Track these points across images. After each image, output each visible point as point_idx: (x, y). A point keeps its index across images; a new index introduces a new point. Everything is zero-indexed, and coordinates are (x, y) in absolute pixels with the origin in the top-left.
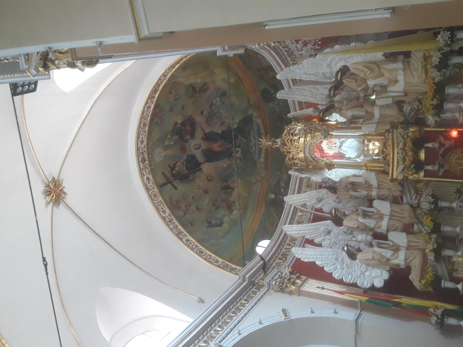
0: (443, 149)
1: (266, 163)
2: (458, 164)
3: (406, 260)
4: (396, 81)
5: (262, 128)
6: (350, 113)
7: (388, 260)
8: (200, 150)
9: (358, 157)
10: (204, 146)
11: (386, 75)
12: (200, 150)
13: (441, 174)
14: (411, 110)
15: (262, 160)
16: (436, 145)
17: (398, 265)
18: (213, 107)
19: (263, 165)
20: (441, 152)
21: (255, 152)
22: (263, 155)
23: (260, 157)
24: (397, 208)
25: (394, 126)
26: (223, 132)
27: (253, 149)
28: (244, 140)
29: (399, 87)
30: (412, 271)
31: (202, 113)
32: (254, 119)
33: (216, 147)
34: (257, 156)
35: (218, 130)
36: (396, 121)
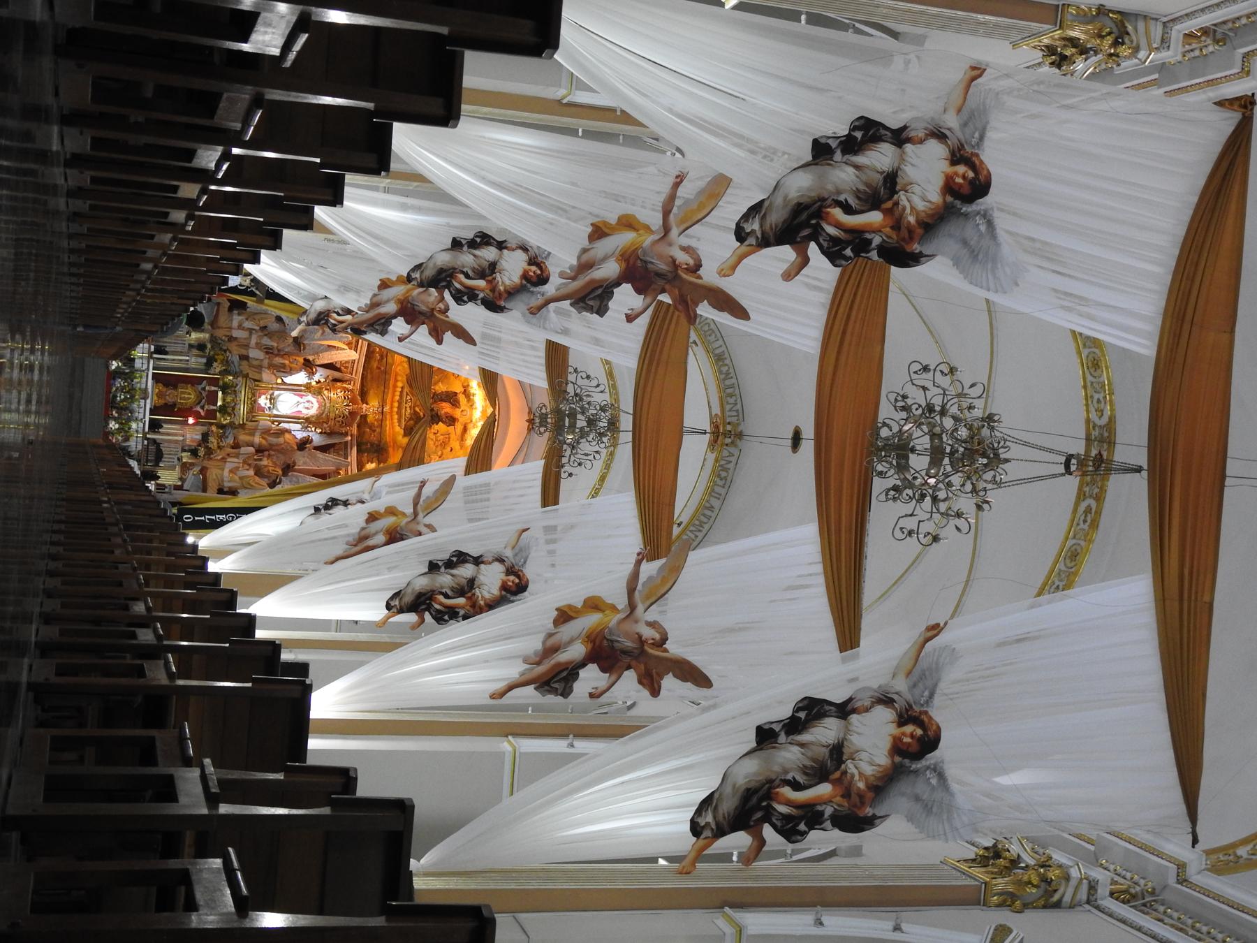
0: (202, 404)
1: (396, 381)
2: (190, 394)
3: (232, 320)
4: (231, 471)
5: (396, 421)
6: (281, 440)
7: (247, 319)
8: (462, 409)
9: (279, 395)
10: (457, 413)
11: (236, 478)
12: (462, 409)
13: (205, 382)
14: (227, 437)
15: (400, 384)
16: (206, 407)
17: (239, 314)
18: (439, 453)
19: (399, 378)
20: (204, 401)
21: (407, 394)
22: (399, 390)
23: (402, 388)
24: (244, 352)
25: (243, 426)
26: (437, 424)
27: (409, 398)
28: (417, 409)
29: (231, 463)
30: (227, 309)
31: (451, 450)
32: (402, 432)
33: (446, 408)
34: (405, 390)
35: (441, 427)
36: (240, 430)
